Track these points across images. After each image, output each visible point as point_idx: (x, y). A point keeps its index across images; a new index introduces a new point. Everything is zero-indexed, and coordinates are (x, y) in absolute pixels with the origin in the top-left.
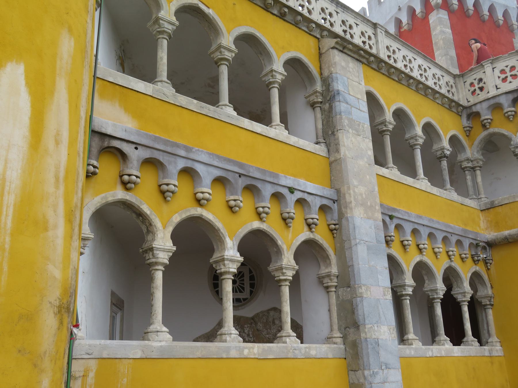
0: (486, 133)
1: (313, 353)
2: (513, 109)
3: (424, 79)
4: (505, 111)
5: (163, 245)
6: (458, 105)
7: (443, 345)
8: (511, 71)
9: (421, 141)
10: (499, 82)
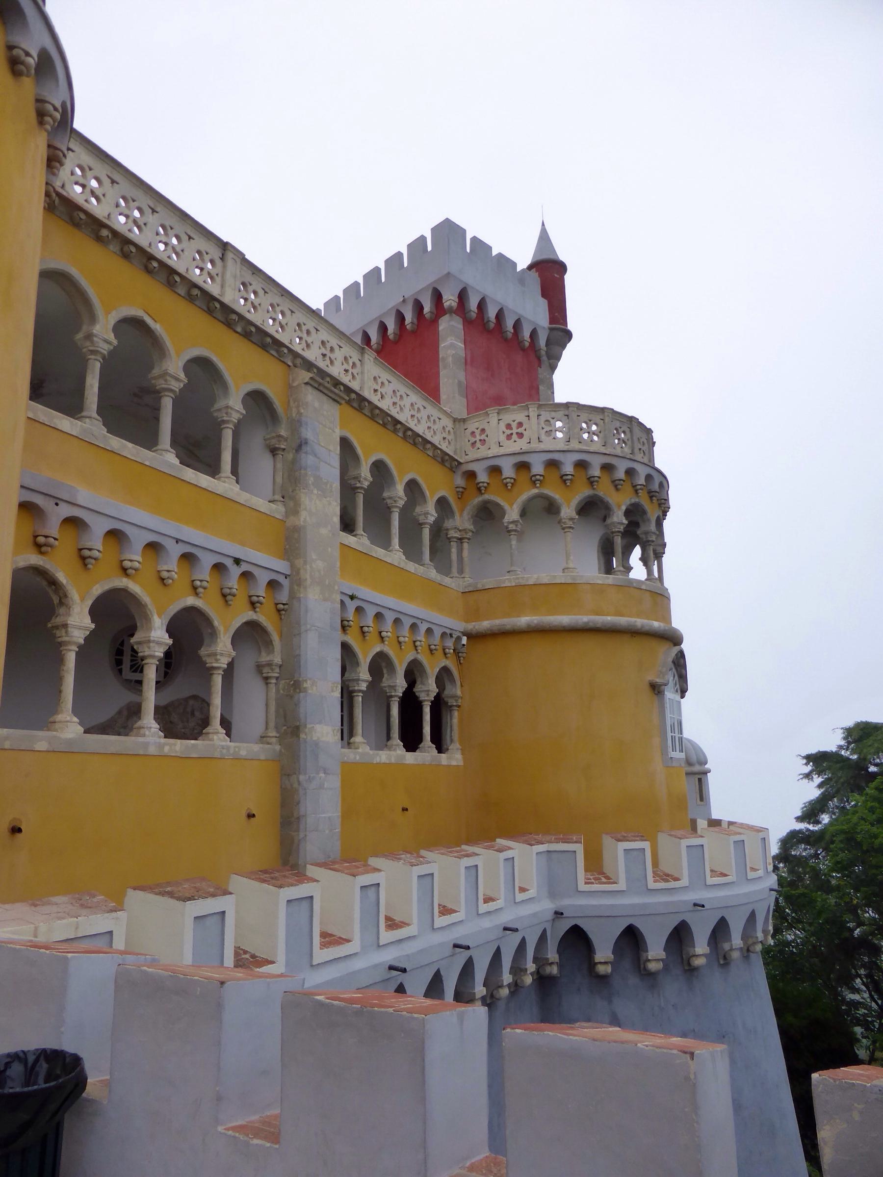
0: (480, 499)
1: (243, 753)
5: (78, 623)
7: (395, 750)
9: (401, 503)
10: (502, 438)
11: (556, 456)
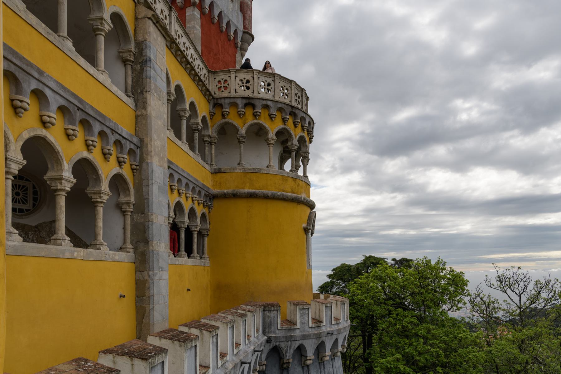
0: (224, 121)
2: (244, 110)
4: (239, 110)
6: (210, 94)
7: (183, 257)
8: (246, 83)
9: (187, 115)
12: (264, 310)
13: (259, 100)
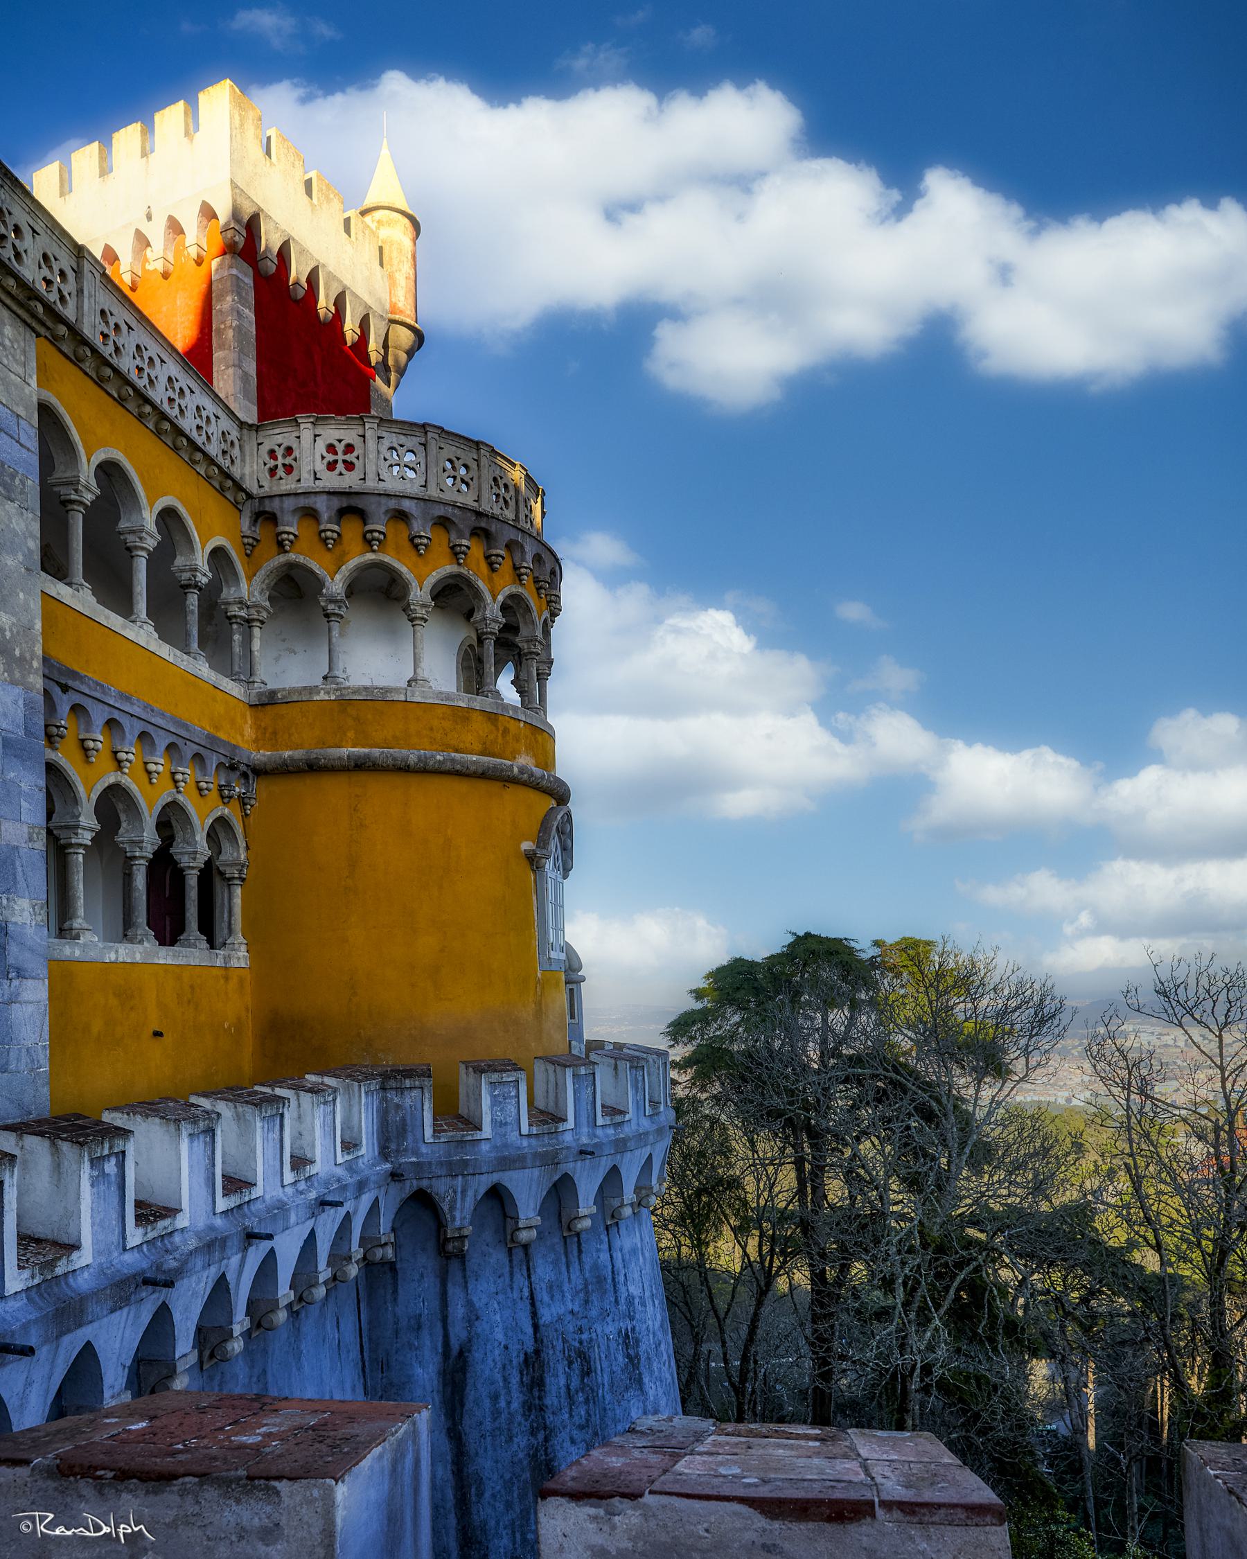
0: (282, 559)
2: (336, 528)
3: (176, 411)
4: (322, 527)
6: (238, 487)
8: (345, 453)
9: (151, 543)
10: (320, 467)
11: (407, 505)
12: (383, 1089)
13: (377, 498)
